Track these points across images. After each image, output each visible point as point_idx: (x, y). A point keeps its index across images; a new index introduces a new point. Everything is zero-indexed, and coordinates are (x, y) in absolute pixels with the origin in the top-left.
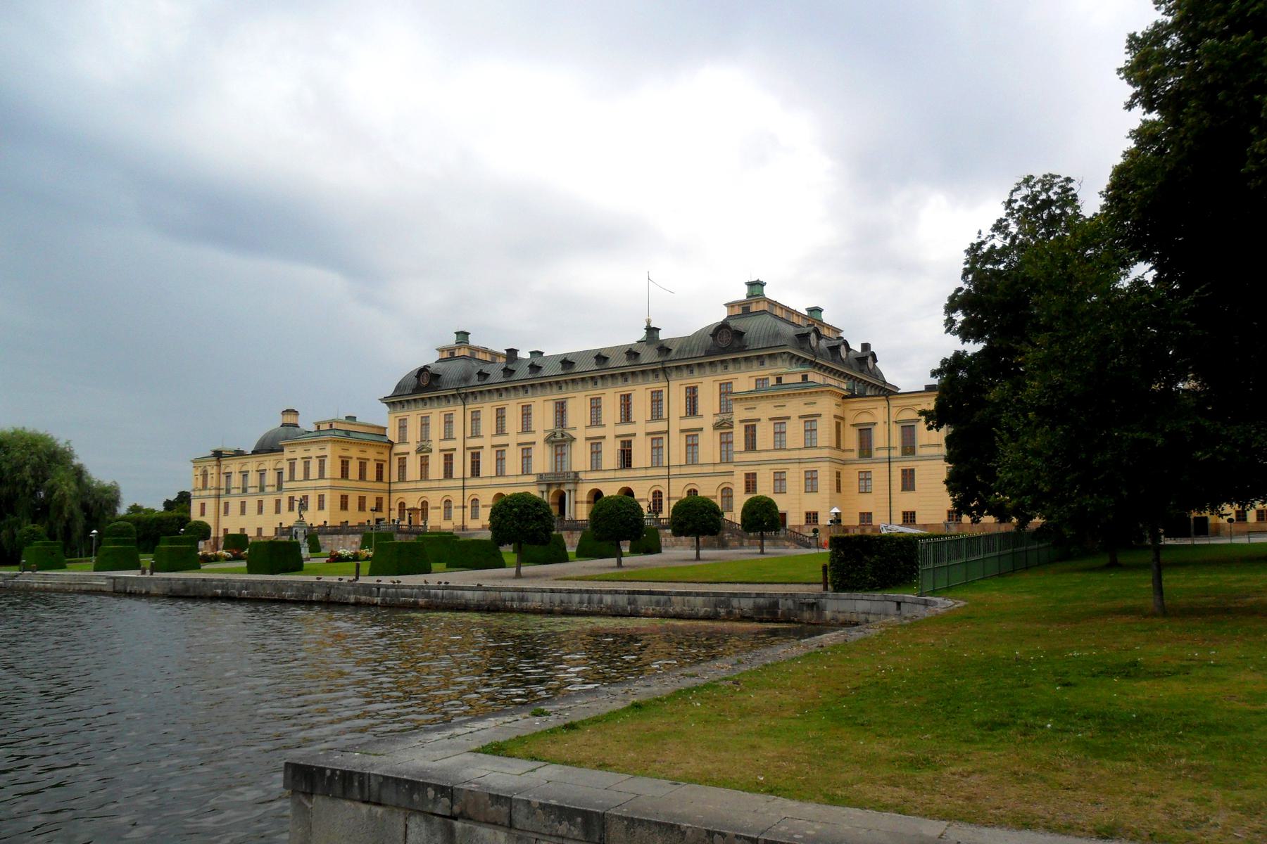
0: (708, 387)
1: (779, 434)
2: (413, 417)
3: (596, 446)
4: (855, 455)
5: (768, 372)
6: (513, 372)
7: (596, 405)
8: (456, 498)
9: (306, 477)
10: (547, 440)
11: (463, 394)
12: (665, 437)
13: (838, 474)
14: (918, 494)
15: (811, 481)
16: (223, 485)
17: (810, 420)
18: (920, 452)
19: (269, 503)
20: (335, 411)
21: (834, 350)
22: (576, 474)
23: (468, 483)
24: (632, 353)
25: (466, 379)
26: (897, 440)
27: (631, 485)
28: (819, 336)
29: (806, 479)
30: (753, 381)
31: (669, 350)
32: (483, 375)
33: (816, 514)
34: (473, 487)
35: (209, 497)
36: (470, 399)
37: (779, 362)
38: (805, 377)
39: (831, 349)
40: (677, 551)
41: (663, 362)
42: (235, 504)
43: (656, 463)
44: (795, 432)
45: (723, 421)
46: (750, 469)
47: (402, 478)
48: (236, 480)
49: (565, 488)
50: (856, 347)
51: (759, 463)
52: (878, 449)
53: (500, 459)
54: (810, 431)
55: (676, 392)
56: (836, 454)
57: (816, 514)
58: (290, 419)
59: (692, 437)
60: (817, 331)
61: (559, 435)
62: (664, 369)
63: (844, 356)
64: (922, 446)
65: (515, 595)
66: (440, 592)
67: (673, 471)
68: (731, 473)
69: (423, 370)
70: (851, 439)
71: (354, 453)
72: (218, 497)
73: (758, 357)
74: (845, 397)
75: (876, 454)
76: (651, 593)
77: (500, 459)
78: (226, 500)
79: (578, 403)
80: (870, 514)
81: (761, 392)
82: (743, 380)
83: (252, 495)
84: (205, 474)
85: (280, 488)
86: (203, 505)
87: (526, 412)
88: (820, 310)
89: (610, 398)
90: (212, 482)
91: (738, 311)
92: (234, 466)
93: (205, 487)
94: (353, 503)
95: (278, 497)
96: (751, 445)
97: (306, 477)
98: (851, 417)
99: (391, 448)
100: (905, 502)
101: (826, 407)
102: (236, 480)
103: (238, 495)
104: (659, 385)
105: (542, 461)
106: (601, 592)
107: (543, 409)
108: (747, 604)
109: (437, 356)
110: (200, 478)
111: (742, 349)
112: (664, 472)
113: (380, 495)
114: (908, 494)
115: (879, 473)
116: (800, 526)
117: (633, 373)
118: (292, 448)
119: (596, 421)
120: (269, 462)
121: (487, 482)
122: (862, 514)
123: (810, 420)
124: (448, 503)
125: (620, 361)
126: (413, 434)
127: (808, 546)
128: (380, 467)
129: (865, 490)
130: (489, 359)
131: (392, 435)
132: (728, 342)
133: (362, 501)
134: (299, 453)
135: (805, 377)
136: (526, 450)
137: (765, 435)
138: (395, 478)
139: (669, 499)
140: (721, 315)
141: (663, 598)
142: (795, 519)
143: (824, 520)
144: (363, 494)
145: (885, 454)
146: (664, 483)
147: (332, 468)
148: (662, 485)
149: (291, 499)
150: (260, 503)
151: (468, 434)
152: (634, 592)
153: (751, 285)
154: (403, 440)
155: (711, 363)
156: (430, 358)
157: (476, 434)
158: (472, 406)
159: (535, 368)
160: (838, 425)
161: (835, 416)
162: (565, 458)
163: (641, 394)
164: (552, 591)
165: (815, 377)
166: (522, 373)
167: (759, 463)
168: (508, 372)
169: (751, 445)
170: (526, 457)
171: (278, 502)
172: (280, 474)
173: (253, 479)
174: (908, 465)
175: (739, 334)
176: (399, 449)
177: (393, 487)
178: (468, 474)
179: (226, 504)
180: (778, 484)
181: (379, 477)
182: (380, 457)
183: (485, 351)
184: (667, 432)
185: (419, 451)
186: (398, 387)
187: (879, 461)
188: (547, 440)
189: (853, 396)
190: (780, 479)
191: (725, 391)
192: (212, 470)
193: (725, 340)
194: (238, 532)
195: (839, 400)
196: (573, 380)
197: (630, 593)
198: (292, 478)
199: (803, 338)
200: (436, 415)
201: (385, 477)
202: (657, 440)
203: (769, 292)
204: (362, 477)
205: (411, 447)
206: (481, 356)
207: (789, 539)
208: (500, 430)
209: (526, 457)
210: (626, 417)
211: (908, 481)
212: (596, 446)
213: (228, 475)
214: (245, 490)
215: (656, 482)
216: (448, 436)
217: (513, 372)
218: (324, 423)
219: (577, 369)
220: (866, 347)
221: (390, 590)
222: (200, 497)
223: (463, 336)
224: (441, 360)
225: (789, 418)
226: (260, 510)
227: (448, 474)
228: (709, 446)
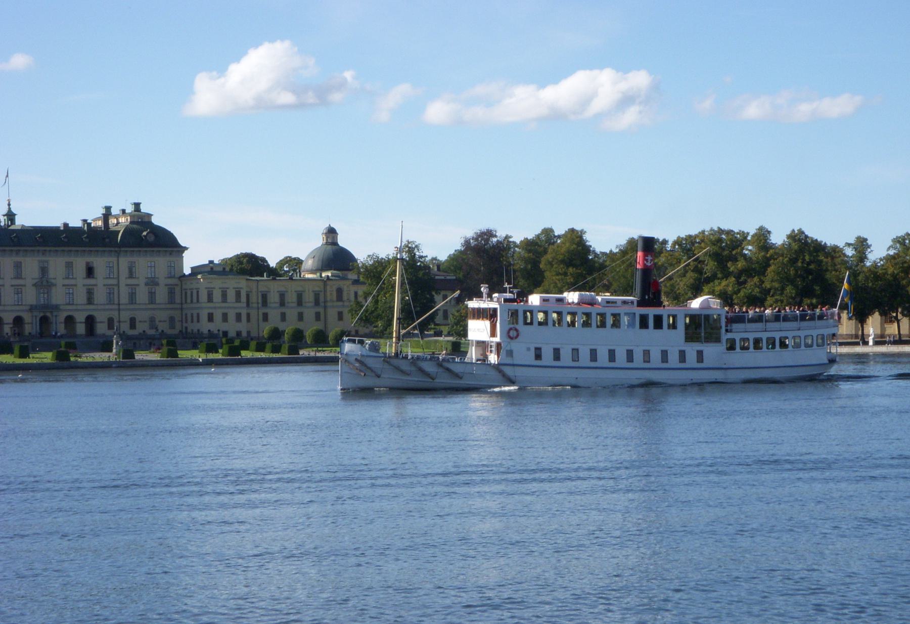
7: (69, 265)
10: (34, 285)
12: (116, 288)
26: (260, 301)
27: (95, 313)
43: (110, 301)
46: (210, 311)
67: (121, 307)
79: (57, 264)
87: (18, 266)
89: (80, 263)
104: (114, 259)
105: (31, 297)
107: (31, 265)
112: (116, 307)
136: (18, 290)
137: (217, 296)
139: (119, 322)
143: (244, 334)
145: (255, 305)
146: (116, 313)
148: (114, 314)
167: (215, 308)
184: (118, 285)
211: (265, 317)
228: (142, 295)
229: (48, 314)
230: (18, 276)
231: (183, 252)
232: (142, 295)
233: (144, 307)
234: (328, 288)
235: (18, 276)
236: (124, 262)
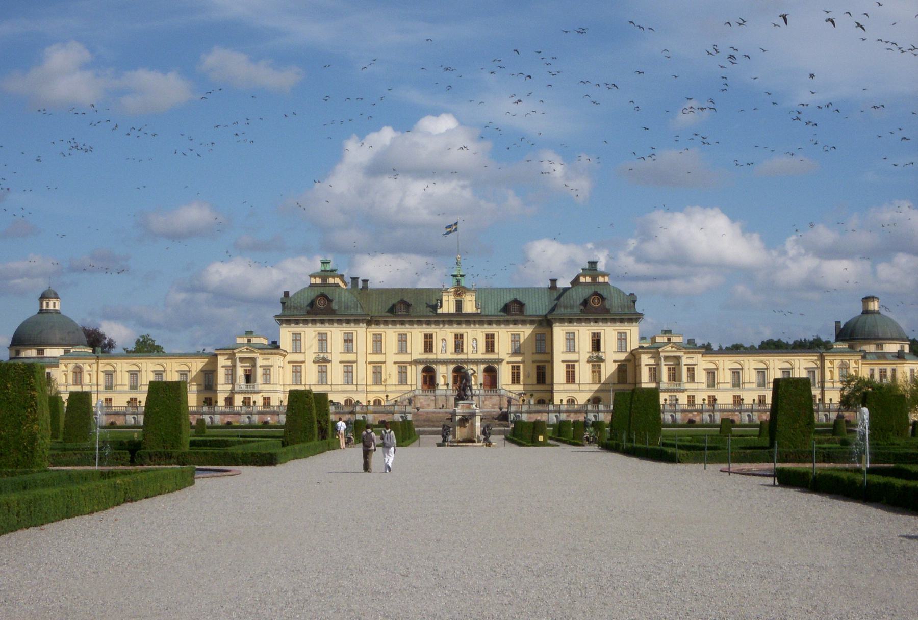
2: (310, 333)
4: (704, 386)
67: (555, 387)
78: (109, 396)
82: (609, 333)
99: (285, 356)
154: (297, 350)
200: (336, 333)
213: (109, 374)
216: (348, 350)
228: (584, 372)
231: (637, 320)
232: (584, 372)
234: (827, 364)
236: (559, 332)
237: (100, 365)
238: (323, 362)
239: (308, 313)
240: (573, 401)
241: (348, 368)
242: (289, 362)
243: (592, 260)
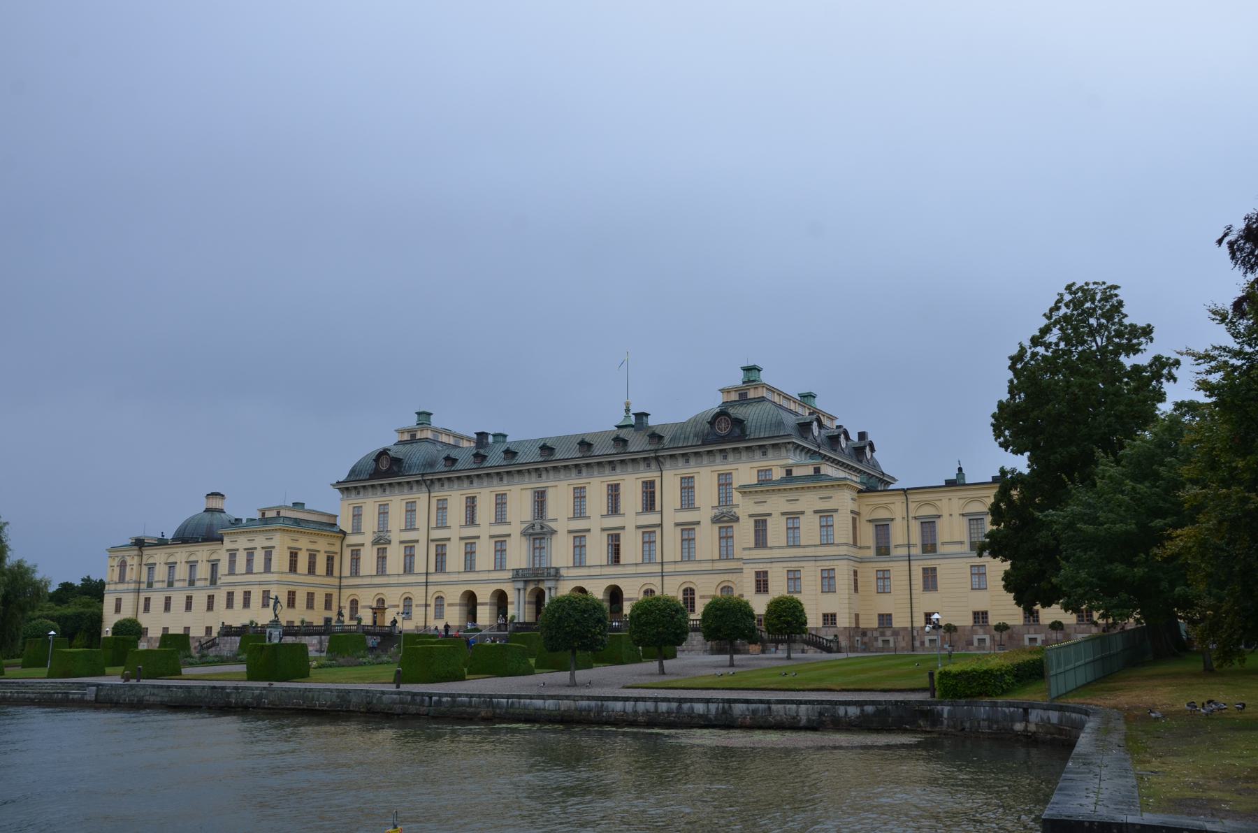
0: (706, 477)
1: (793, 529)
2: (370, 505)
3: (579, 538)
4: (871, 553)
5: (776, 466)
6: (484, 457)
7: (579, 495)
8: (418, 595)
9: (249, 571)
10: (524, 534)
11: (429, 484)
12: (658, 530)
13: (855, 572)
14: (971, 593)
15: (828, 580)
16: (144, 578)
17: (826, 515)
18: (941, 549)
19: (200, 599)
20: (278, 497)
21: (833, 440)
22: (557, 569)
23: (431, 578)
24: (620, 441)
25: (431, 464)
26: (916, 538)
27: (620, 583)
28: (821, 425)
29: (823, 578)
30: (755, 471)
31: (661, 438)
32: (451, 460)
33: (834, 616)
34: (437, 583)
35: (127, 591)
36: (437, 486)
37: (783, 453)
38: (817, 470)
39: (829, 437)
40: (695, 658)
41: (656, 451)
42: (157, 600)
43: (648, 559)
44: (809, 528)
45: (723, 515)
46: (761, 567)
47: (355, 572)
48: (161, 573)
49: (544, 586)
50: (854, 437)
51: (771, 561)
52: (896, 546)
53: (470, 554)
54: (826, 527)
55: (669, 482)
56: (853, 551)
57: (834, 616)
58: (215, 503)
59: (687, 530)
60: (819, 421)
61: (537, 527)
62: (657, 458)
63: (844, 445)
64: (943, 544)
65: (593, 703)
66: (504, 700)
67: (667, 568)
68: (740, 571)
69: (383, 453)
70: (868, 535)
71: (304, 543)
72: (138, 591)
73: (760, 447)
74: (860, 491)
75: (895, 552)
76: (747, 701)
77: (470, 554)
78: (147, 595)
79: (560, 493)
80: (890, 615)
81: (764, 484)
82: (745, 471)
83: (180, 589)
84: (123, 565)
85: (213, 581)
86: (119, 601)
87: (501, 502)
88: (810, 396)
89: (596, 487)
90: (130, 575)
91: (734, 397)
92: (159, 557)
93: (122, 579)
94: (301, 599)
95: (211, 592)
96: (761, 539)
97: (249, 571)
98: (867, 513)
100: (925, 602)
101: (844, 501)
102: (161, 573)
103: (162, 590)
104: (652, 475)
105: (519, 555)
106: (691, 700)
107: (520, 498)
108: (853, 711)
109: (397, 438)
110: (117, 570)
111: (742, 437)
112: (657, 569)
113: (329, 591)
114: (930, 596)
115: (898, 571)
116: (817, 629)
117: (622, 462)
118: (233, 538)
119: (579, 511)
120: (202, 553)
121: (454, 578)
122: (881, 616)
123: (826, 515)
124: (408, 600)
125: (604, 448)
126: (370, 523)
127: (829, 650)
128: (330, 559)
129: (883, 590)
130: (452, 441)
131: (345, 523)
132: (726, 432)
133: (310, 596)
134: (242, 543)
135: (817, 470)
136: (500, 544)
137: (777, 531)
138: (347, 571)
140: (713, 402)
141: (762, 706)
142: (814, 621)
143: (843, 621)
144: (311, 590)
147: (280, 560)
149: (230, 596)
150: (189, 599)
151: (433, 524)
152: (730, 701)
153: (747, 370)
154: (357, 530)
155: (709, 452)
156: (388, 439)
157: (442, 525)
158: (438, 493)
159: (510, 453)
160: (854, 520)
161: (852, 512)
162: (544, 552)
163: (631, 484)
164: (637, 700)
165: (828, 470)
166: (495, 457)
167: (771, 561)
168: (480, 457)
169: (761, 539)
170: (500, 550)
171: (211, 598)
172: (214, 567)
173: (182, 572)
174: (929, 563)
175: (739, 422)
176: (352, 539)
177: (344, 582)
178: (432, 569)
179: (147, 600)
180: (792, 583)
181: (330, 572)
182: (332, 549)
183: (448, 433)
184: (661, 525)
185: (375, 543)
186: (353, 472)
187: (898, 559)
188: (524, 534)
189: (868, 490)
190: (794, 577)
191: (725, 482)
192: (133, 561)
193: (723, 428)
194: (181, 632)
195: (855, 495)
196: (555, 468)
197: (724, 701)
198: (232, 572)
199: (804, 428)
200: (397, 503)
201: (336, 572)
202: (649, 535)
203: (764, 377)
204: (312, 570)
205: (367, 538)
206: (444, 439)
207: (808, 643)
208: (471, 520)
209: (500, 550)
210: (614, 508)
212: (579, 538)
213: (151, 567)
214: (170, 584)
215: (648, 580)
216: (410, 527)
217: (484, 457)
218: (270, 509)
219: (558, 456)
220: (862, 436)
221: (444, 699)
222: (115, 591)
223: (424, 416)
224: (400, 443)
225: (802, 513)
226: (189, 607)
227: (409, 569)
229: (541, 586)
230: (500, 519)
233: (708, 566)
235: (500, 519)
237: (145, 557)
238: (381, 542)
239: (372, 477)
240: (692, 591)
241: (409, 547)
242: (348, 546)
243: (751, 364)
